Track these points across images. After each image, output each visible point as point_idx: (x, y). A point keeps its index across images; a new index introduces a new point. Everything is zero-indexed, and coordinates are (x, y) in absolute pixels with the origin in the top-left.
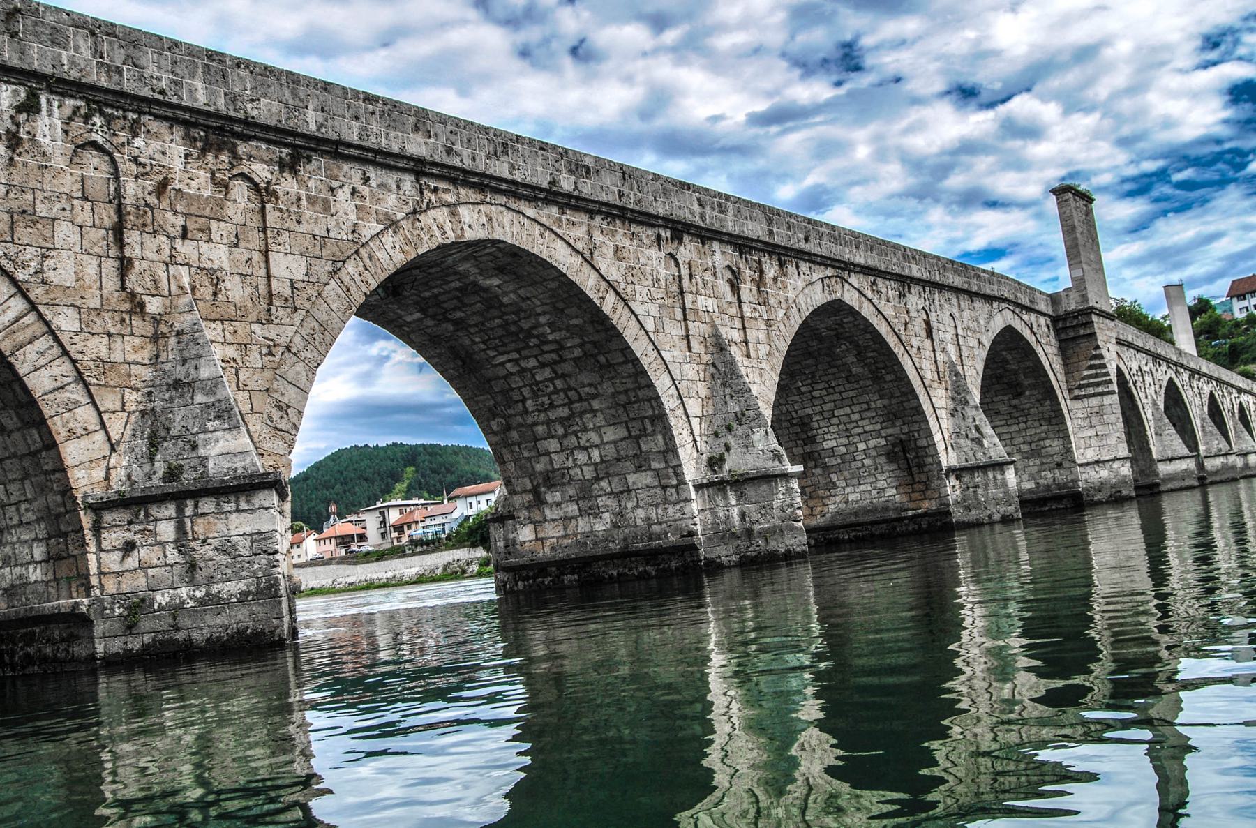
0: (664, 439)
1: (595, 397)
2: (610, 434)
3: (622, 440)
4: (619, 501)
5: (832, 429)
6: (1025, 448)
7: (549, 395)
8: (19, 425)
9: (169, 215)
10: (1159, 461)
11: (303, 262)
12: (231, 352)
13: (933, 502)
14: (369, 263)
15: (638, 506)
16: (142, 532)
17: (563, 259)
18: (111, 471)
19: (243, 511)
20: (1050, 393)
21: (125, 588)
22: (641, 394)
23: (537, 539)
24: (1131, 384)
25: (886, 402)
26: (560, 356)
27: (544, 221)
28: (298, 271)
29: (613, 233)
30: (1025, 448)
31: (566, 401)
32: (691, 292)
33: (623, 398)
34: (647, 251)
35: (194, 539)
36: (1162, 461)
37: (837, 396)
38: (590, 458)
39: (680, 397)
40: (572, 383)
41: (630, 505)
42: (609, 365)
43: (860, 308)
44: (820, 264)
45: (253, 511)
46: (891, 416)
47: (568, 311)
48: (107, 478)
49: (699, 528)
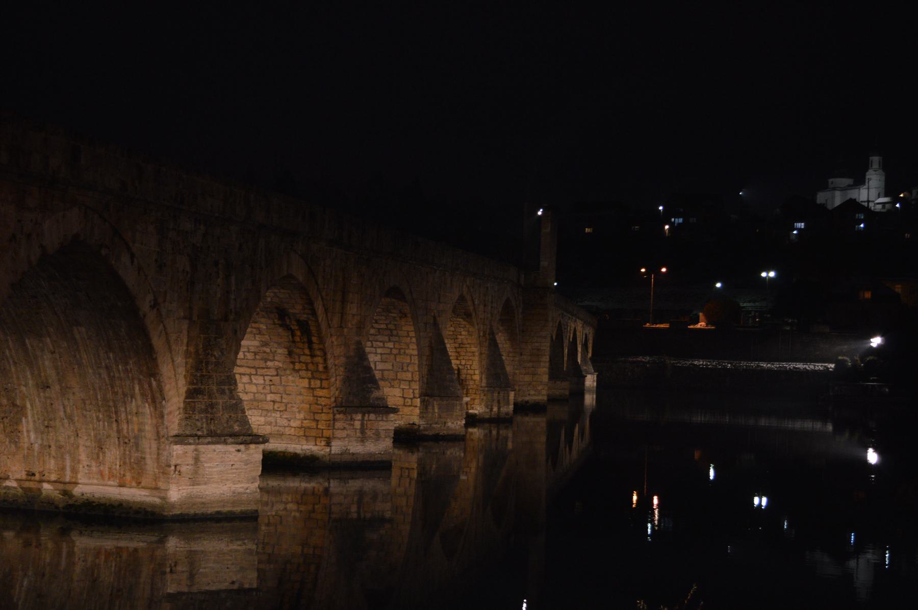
8: (310, 377)
19: (384, 421)
45: (387, 421)
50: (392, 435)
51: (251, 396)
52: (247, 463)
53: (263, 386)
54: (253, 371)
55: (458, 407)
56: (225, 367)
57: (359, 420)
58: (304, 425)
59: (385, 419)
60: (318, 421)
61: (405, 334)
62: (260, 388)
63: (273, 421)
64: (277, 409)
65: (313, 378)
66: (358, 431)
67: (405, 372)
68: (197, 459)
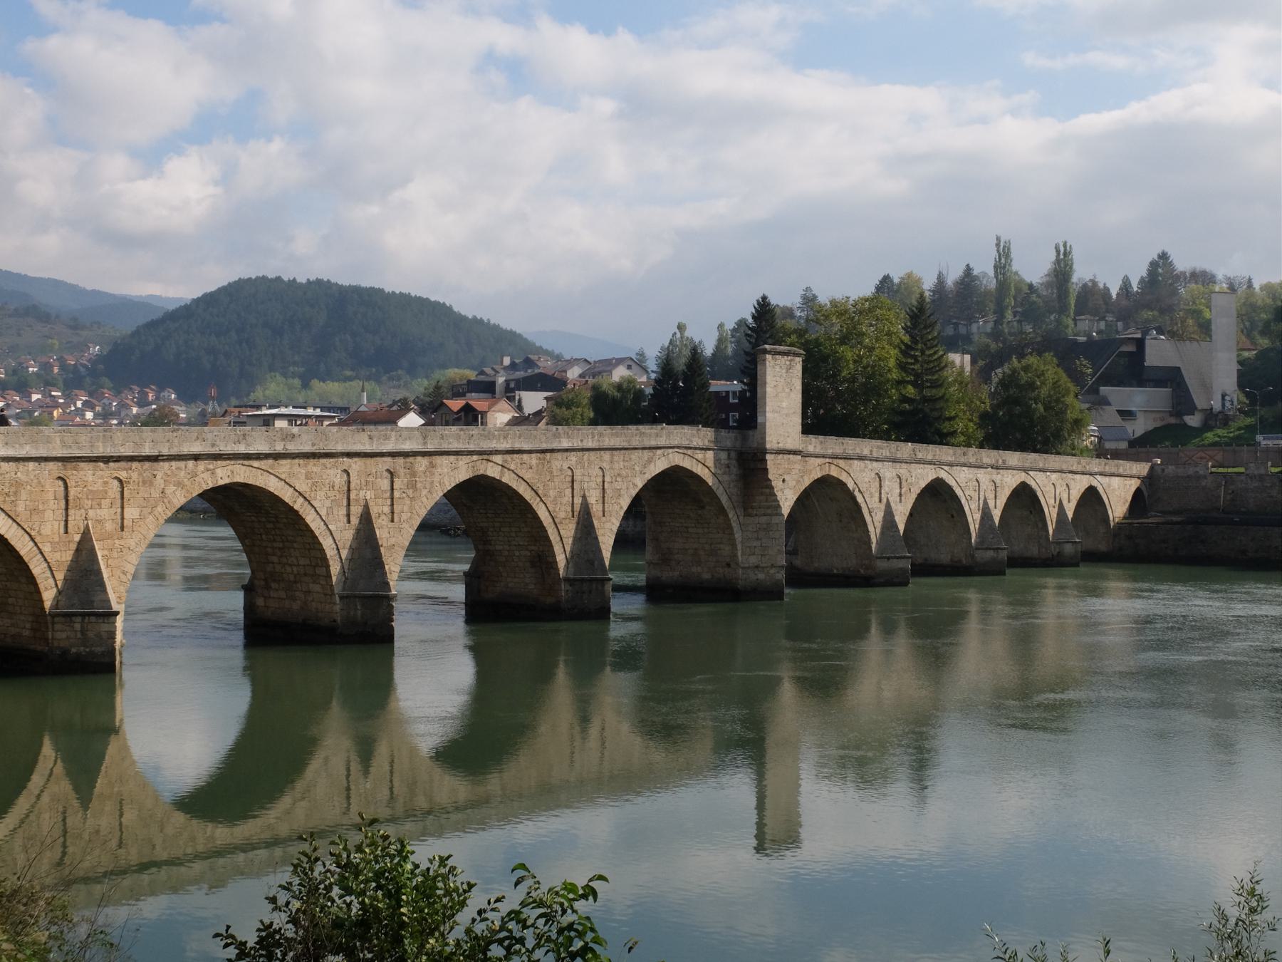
2: (302, 561)
3: (308, 565)
5: (500, 538)
6: (707, 547)
7: (273, 535)
9: (86, 501)
10: (877, 558)
11: (138, 510)
12: (106, 552)
14: (168, 505)
16: (69, 626)
17: (273, 485)
20: (722, 510)
21: (62, 644)
23: (265, 606)
24: (857, 493)
27: (264, 468)
28: (136, 515)
29: (306, 465)
30: (707, 547)
32: (356, 490)
34: (328, 472)
35: (87, 631)
36: (880, 558)
37: (501, 520)
38: (293, 571)
39: (338, 549)
43: (501, 477)
44: (468, 455)
45: (108, 623)
49: (339, 619)
59: (106, 621)
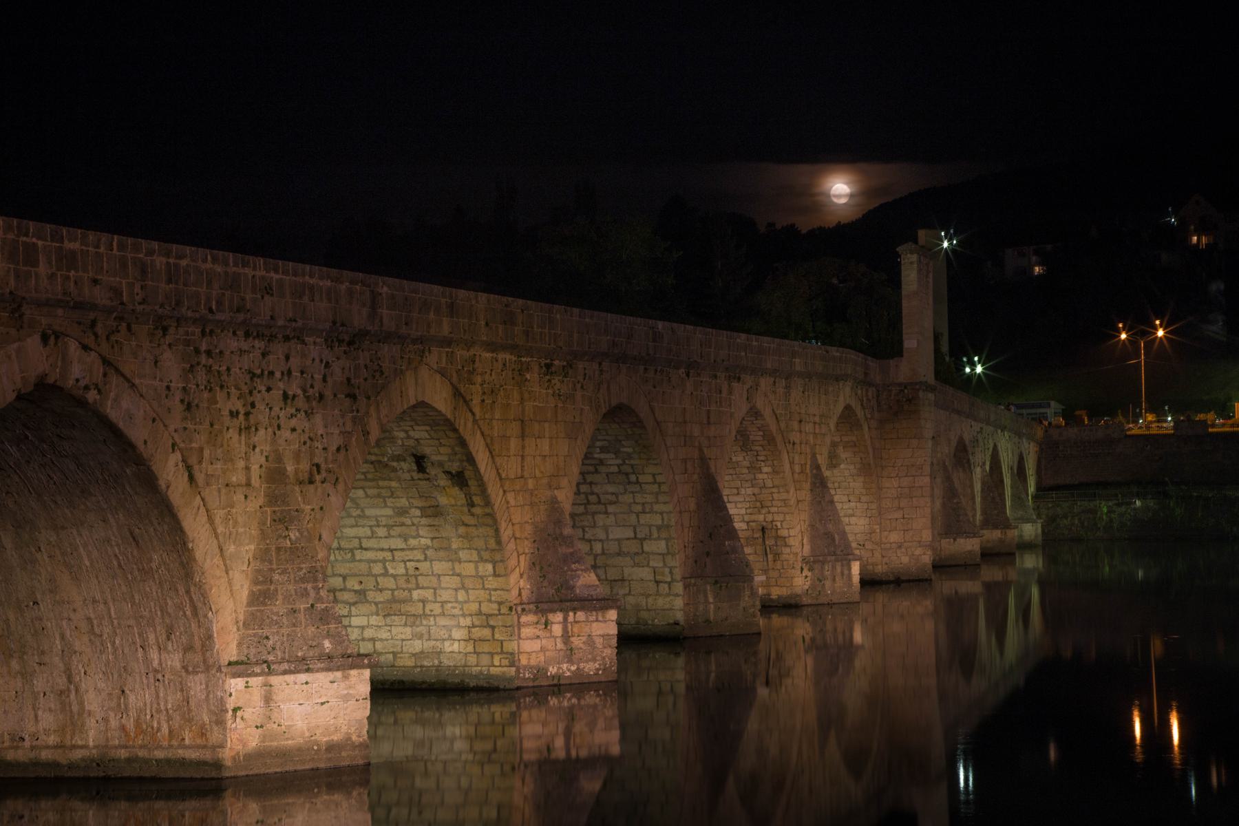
0: (667, 545)
1: (611, 503)
3: (628, 539)
4: (611, 588)
8: (477, 559)
13: (785, 589)
15: (629, 594)
18: (522, 590)
19: (600, 621)
21: (533, 662)
22: (657, 507)
25: (756, 491)
26: (596, 470)
31: (585, 501)
33: (639, 508)
35: (573, 636)
38: (591, 549)
40: (596, 489)
41: (622, 592)
42: (637, 482)
45: (605, 621)
46: (758, 504)
47: (623, 442)
48: (520, 594)
50: (614, 642)
51: (387, 595)
52: (346, 698)
53: (405, 578)
54: (388, 555)
55: (747, 593)
56: (307, 555)
57: (560, 623)
58: (473, 636)
59: (600, 618)
60: (493, 628)
61: (649, 479)
62: (402, 582)
63: (423, 632)
64: (429, 613)
65: (482, 560)
66: (559, 640)
67: (655, 539)
68: (268, 699)
